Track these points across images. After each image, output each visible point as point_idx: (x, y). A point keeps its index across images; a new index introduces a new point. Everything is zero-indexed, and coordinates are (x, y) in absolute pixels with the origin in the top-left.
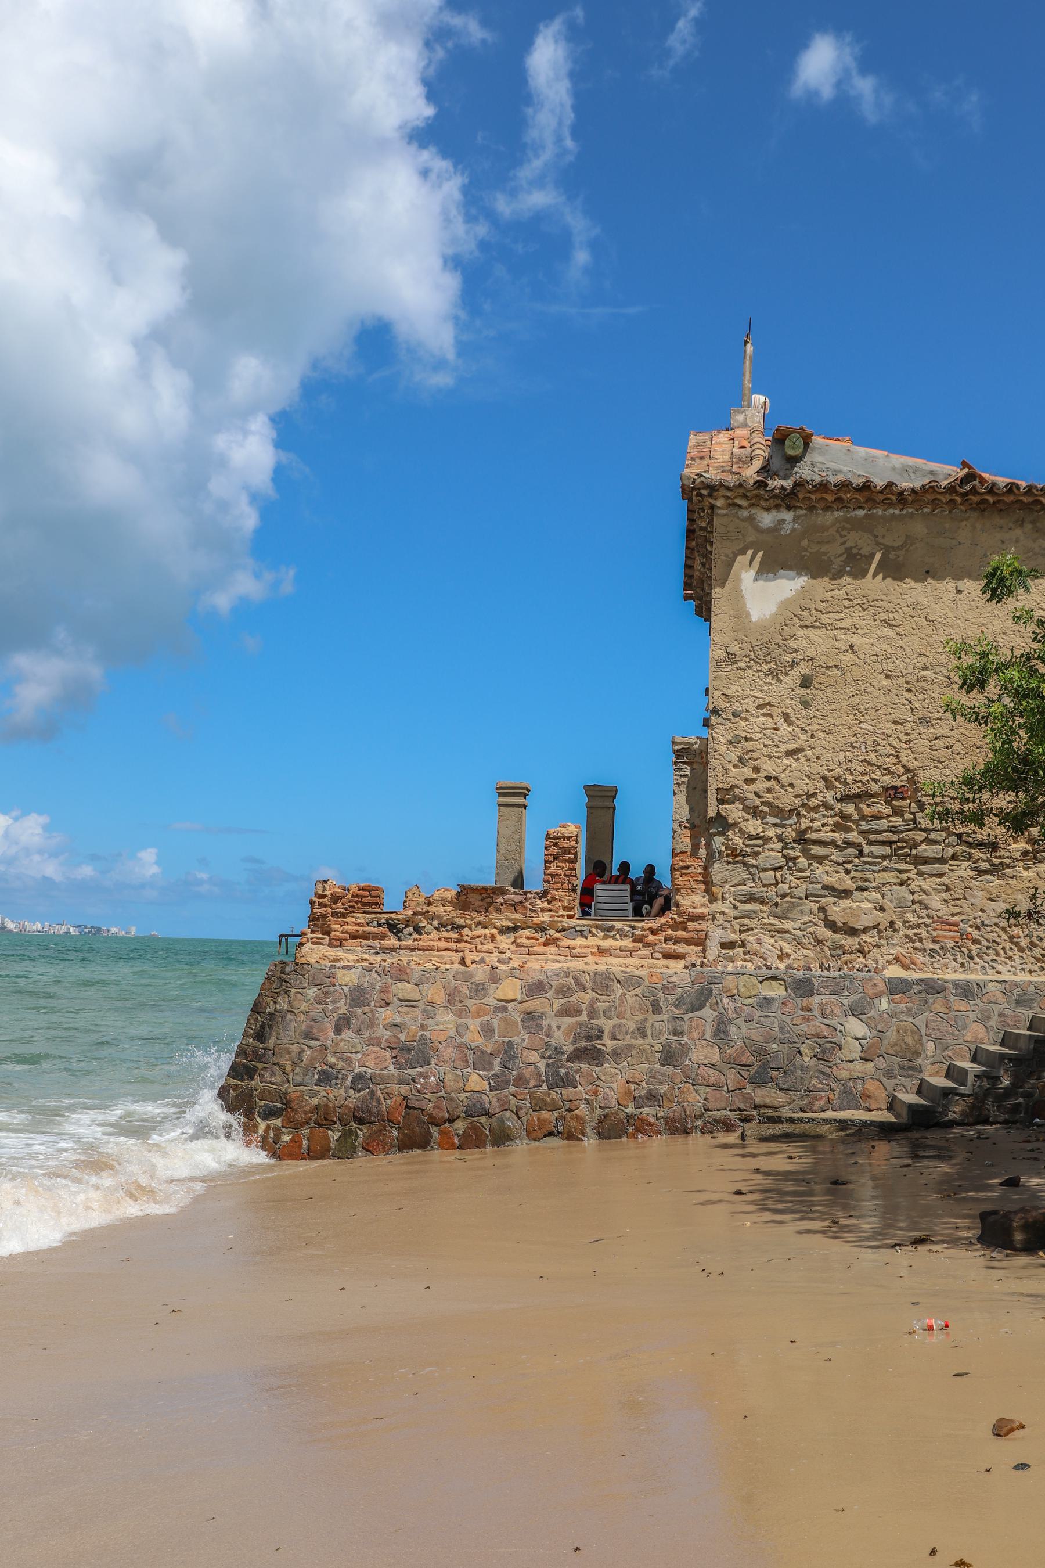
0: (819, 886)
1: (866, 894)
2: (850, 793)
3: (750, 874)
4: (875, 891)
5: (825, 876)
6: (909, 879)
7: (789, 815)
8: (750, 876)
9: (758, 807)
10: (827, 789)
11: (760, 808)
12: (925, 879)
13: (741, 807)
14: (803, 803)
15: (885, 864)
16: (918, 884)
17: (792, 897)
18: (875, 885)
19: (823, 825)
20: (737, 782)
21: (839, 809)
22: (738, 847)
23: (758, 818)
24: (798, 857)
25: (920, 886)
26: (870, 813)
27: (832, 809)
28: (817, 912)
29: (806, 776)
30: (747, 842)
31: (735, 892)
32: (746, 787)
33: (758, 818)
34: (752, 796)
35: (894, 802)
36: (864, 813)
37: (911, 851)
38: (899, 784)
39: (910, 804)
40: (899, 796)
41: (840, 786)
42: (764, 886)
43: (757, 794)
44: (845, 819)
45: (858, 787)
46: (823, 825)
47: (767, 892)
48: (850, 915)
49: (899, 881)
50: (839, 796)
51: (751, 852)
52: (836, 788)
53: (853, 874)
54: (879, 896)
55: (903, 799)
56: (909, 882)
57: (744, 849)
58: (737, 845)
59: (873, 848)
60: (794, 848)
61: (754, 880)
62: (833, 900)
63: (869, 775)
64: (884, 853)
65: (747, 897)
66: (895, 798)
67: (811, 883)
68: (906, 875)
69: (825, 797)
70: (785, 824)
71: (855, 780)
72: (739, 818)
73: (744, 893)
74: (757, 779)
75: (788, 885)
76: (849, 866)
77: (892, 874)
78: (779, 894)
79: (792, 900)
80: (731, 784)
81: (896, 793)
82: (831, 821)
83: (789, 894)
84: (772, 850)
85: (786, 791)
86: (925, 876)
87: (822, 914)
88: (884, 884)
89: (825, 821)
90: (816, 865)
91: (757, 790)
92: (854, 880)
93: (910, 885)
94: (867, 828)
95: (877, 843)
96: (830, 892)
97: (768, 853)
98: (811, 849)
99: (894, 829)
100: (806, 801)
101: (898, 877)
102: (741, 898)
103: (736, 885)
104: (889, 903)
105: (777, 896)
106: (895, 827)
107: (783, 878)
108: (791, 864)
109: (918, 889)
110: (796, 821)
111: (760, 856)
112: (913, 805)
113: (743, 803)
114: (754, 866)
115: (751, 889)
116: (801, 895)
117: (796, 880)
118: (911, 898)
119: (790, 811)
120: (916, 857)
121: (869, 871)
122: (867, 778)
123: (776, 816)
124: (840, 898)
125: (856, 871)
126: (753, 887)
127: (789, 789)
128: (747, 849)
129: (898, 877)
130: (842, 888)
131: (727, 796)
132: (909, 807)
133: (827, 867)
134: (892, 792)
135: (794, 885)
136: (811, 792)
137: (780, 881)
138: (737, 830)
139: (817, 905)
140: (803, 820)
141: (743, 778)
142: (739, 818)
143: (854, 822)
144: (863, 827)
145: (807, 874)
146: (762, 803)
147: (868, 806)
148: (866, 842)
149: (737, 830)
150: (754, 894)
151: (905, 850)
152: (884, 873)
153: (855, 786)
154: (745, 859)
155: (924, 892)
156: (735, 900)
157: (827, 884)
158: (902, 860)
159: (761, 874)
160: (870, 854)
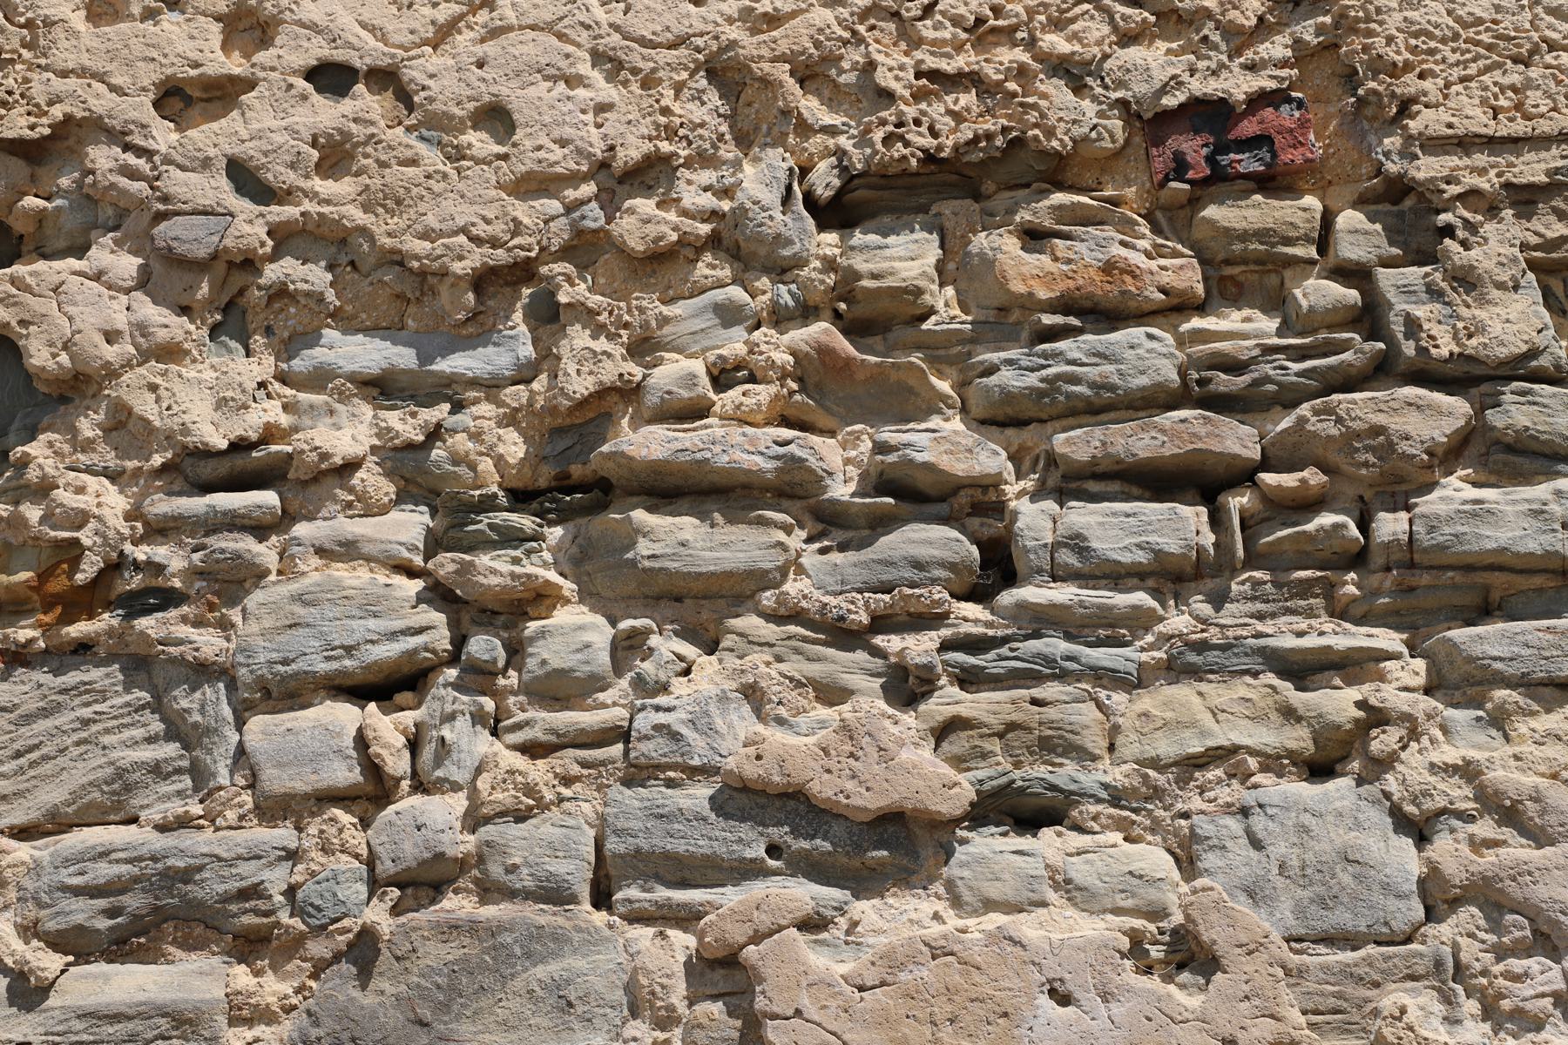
0: (698, 795)
1: (1050, 843)
2: (899, 150)
3: (172, 734)
4: (1122, 825)
5: (742, 722)
6: (1375, 717)
7: (474, 316)
8: (171, 749)
9: (249, 263)
10: (744, 141)
11: (272, 273)
12: (1499, 721)
13: (127, 265)
14: (579, 233)
15: (1178, 622)
16: (1450, 754)
17: (488, 891)
18: (1118, 775)
19: (723, 377)
20: (101, 101)
21: (830, 265)
22: (86, 537)
23: (258, 340)
24: (540, 599)
25: (1467, 771)
26: (1048, 278)
27: (782, 271)
28: (677, 995)
29: (598, 57)
30: (162, 505)
31: (36, 868)
32: (164, 136)
33: (258, 340)
34: (216, 189)
35: (1211, 212)
36: (1002, 282)
37: (1364, 525)
38: (1238, 85)
39: (1328, 219)
40: (1248, 163)
41: (829, 119)
42: (272, 809)
43: (244, 176)
44: (875, 339)
45: (958, 117)
46: (723, 377)
47: (293, 856)
48: (942, 1009)
49: (1298, 739)
50: (824, 180)
51: (195, 573)
52: (805, 129)
53: (948, 700)
54: (1154, 858)
55: (1273, 183)
56: (1384, 741)
57: (141, 553)
58: (80, 519)
59: (1083, 516)
60: (510, 538)
61: (199, 775)
62: (804, 893)
63: (1031, 44)
64: (1171, 545)
65: (134, 902)
66: (1218, 181)
67: (638, 774)
68: (1354, 694)
69: (726, 192)
70: (451, 380)
71: (934, 75)
72: (111, 337)
73: (104, 871)
74: (250, 84)
75: (459, 802)
76: (919, 647)
77: (1242, 688)
78: (386, 867)
79: (490, 912)
80: (57, 112)
81: (1222, 148)
82: (778, 347)
83: (462, 864)
84: (348, 551)
85: (457, 155)
86: (1501, 694)
87: (716, 1008)
88: (1192, 764)
89: (734, 344)
90: (667, 645)
91: (250, 150)
92: (959, 743)
93: (1385, 763)
94: (1032, 380)
95: (1115, 487)
96: (779, 833)
97: (312, 573)
98: (635, 533)
99: (1224, 382)
100: (594, 216)
101: (1289, 714)
102: (82, 912)
103: (54, 824)
104: (1242, 906)
105: (375, 884)
106: (1234, 366)
107: (428, 753)
108: (484, 646)
109: (1459, 794)
110: (527, 351)
111: (254, 599)
112: (1349, 218)
113: (140, 243)
114: (202, 672)
115: (159, 842)
116: (560, 867)
117: (519, 761)
118: (1405, 861)
119: (483, 280)
120: (1411, 565)
121: (1063, 676)
122: (1009, 56)
123: (389, 329)
124: (864, 883)
125: (969, 680)
126: (184, 823)
127: (479, 142)
128: (160, 552)
129: (1289, 714)
130: (869, 801)
131: (30, 202)
132: (1324, 237)
133: (758, 657)
134: (1194, 148)
135: (504, 797)
136: (632, 151)
137: (397, 763)
138: (87, 427)
139: (683, 941)
140: (579, 338)
141: (149, 76)
142: (111, 337)
143: (943, 351)
144: (1007, 378)
145: (610, 708)
146: (285, 239)
147: (1034, 237)
148: (1028, 484)
149: (87, 427)
150: (186, 875)
151: (1327, 519)
152: (1184, 693)
153: (936, 110)
154: (147, 624)
155: (1509, 814)
156: (29, 931)
157: (752, 771)
158: (1305, 588)
159: (256, 723)
160: (1067, 557)
